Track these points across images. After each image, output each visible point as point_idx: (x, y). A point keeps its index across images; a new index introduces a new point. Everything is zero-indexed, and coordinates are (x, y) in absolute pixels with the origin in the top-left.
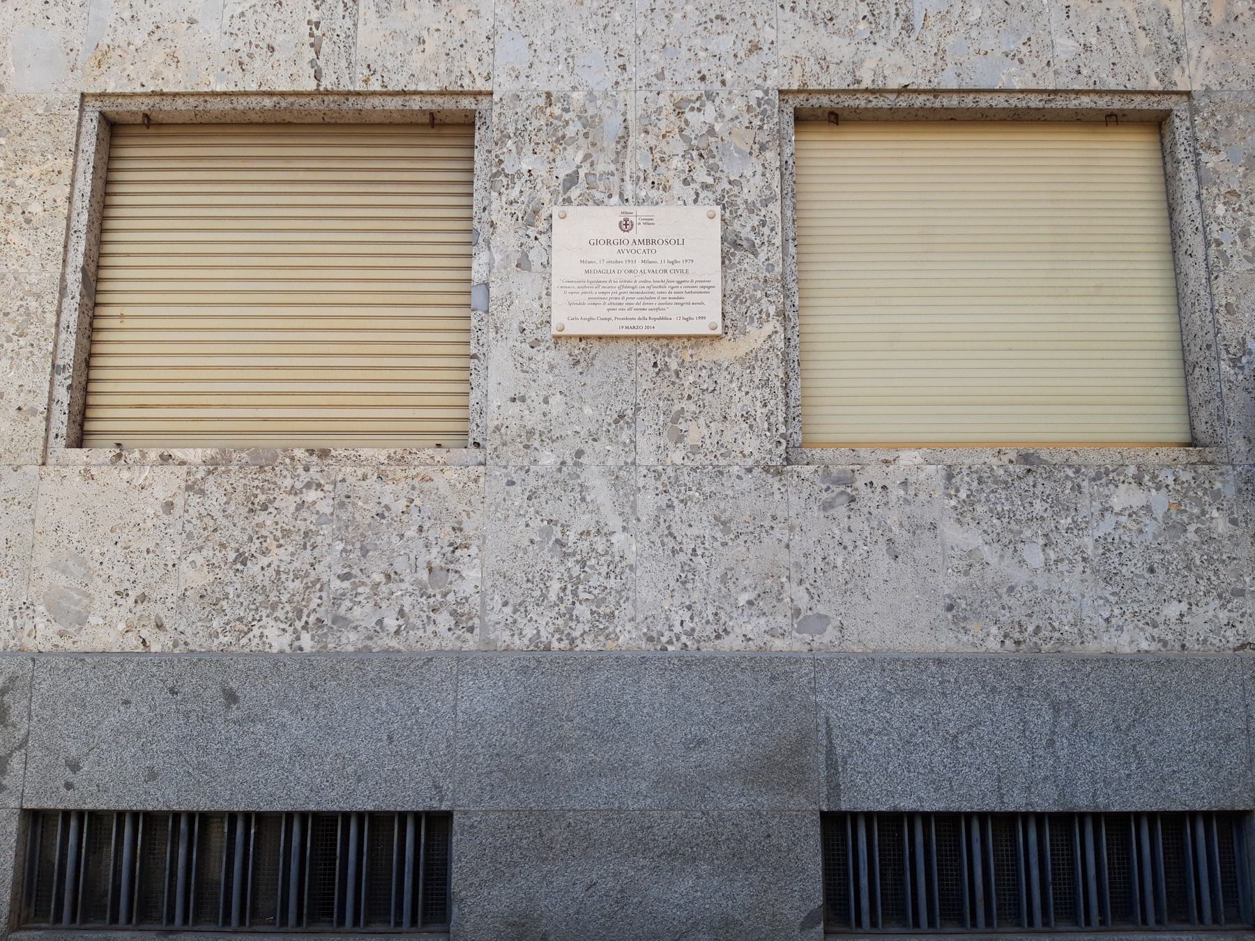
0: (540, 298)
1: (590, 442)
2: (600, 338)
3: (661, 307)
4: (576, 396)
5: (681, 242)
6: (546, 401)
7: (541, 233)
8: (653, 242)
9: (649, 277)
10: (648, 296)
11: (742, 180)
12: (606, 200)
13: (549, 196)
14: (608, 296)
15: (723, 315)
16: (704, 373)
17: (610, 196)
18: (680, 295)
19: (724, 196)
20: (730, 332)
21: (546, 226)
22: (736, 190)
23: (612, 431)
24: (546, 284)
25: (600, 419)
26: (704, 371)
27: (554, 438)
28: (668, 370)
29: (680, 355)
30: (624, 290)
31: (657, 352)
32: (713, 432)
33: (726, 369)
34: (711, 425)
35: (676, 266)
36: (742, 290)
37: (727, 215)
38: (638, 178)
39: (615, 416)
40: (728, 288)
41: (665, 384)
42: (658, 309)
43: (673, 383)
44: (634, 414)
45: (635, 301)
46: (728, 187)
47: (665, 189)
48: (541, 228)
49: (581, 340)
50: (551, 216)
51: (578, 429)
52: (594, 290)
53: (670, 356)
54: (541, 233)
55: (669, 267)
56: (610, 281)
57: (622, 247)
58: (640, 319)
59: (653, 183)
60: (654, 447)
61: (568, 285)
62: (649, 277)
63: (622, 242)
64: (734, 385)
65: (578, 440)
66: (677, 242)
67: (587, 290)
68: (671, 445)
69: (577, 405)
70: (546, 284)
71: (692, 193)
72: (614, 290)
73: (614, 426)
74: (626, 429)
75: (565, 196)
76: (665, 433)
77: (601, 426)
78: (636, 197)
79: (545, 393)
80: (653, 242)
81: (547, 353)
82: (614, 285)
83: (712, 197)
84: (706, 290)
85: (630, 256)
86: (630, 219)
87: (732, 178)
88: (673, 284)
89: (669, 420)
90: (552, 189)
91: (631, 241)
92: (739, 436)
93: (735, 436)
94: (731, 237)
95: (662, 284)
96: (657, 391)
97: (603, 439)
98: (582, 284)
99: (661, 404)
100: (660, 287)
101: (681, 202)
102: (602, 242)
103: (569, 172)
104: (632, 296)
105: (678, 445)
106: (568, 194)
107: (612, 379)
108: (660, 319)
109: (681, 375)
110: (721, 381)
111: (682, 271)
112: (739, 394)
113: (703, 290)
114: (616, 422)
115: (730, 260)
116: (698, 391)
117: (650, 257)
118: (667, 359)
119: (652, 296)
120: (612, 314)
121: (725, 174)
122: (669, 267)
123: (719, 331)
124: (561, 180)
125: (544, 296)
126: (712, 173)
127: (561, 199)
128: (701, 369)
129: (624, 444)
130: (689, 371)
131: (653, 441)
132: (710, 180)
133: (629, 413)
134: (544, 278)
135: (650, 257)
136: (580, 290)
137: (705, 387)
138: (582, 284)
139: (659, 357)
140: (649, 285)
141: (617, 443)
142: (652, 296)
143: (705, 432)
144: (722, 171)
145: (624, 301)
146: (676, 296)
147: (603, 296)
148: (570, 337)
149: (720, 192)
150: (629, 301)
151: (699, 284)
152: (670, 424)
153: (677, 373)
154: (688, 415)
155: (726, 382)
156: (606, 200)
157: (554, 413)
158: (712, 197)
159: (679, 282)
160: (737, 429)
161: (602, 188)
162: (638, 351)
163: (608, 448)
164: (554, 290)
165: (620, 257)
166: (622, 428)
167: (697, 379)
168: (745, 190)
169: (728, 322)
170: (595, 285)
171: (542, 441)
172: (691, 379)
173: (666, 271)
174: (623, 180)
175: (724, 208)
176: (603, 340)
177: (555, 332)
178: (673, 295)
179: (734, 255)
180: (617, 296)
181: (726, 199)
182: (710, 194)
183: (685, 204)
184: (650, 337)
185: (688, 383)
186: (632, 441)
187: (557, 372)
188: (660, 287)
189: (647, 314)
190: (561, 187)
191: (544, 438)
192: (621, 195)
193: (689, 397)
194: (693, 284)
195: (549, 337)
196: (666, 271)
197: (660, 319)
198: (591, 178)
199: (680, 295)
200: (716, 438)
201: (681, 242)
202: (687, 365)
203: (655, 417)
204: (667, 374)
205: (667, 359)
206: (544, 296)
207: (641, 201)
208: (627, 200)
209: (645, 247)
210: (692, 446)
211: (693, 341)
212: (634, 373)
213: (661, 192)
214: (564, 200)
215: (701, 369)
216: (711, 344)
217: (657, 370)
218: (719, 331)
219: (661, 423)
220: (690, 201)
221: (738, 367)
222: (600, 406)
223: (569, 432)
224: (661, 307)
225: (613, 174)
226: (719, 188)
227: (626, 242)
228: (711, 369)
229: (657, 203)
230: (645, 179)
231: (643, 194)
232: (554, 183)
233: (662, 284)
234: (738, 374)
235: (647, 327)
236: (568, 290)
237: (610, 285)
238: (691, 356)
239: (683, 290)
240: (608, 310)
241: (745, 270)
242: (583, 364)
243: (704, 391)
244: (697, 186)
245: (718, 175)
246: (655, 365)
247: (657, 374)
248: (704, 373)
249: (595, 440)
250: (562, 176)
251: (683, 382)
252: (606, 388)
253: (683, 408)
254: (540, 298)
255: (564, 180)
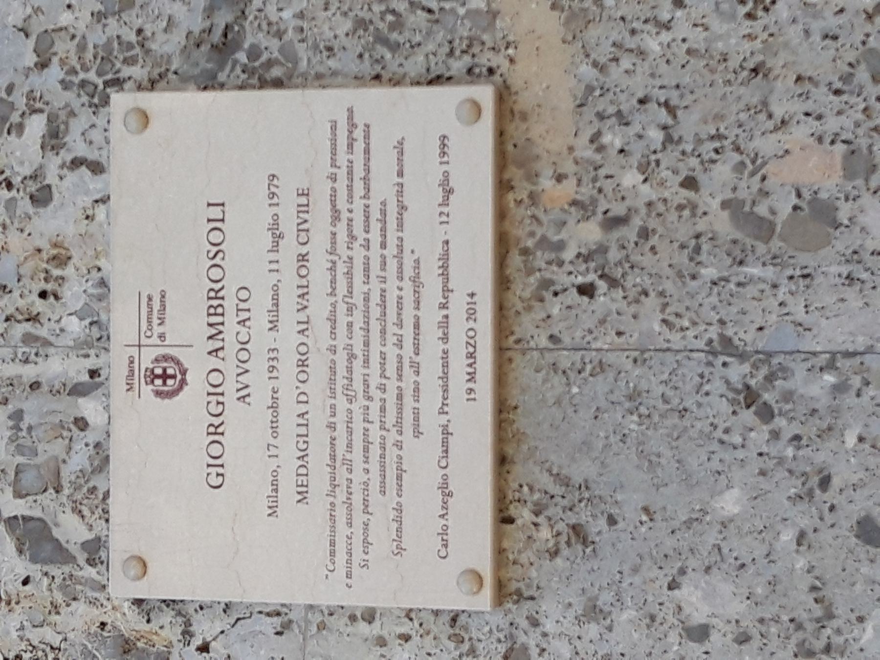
0: (382, 642)
1: (830, 496)
2: (502, 461)
3: (408, 272)
4: (686, 538)
5: (216, 213)
6: (700, 633)
7: (187, 634)
8: (216, 294)
9: (319, 307)
10: (375, 312)
11: (36, 29)
12: (91, 437)
13: (80, 607)
14: (375, 433)
15: (436, 80)
16: (613, 139)
17: (82, 424)
18: (375, 214)
19: (83, 84)
20: (486, 59)
21: (167, 617)
22: (63, 47)
23: (795, 429)
24: (339, 622)
25: (756, 464)
26: (607, 139)
27: (818, 611)
28: (602, 249)
29: (556, 215)
30: (358, 385)
31: (546, 284)
32: (798, 107)
33: (602, 69)
34: (779, 111)
35: (289, 227)
36: (361, 24)
37: (137, 72)
38: (28, 339)
39: (748, 416)
40: (354, 67)
41: (647, 260)
42: (416, 280)
43: (645, 233)
44: (742, 357)
45: (392, 352)
46: (55, 72)
47: (61, 260)
48: (173, 634)
49: (510, 520)
50: (139, 602)
51: (788, 536)
52: (358, 476)
53: (560, 246)
54: (187, 634)
55: (290, 248)
56: (332, 427)
57: (230, 388)
58: (445, 338)
59: (43, 295)
60: (850, 293)
61: (341, 557)
62: (319, 307)
63: (215, 391)
64: (653, 44)
65: (826, 535)
66: (216, 224)
67: (357, 499)
68: (843, 242)
69: (712, 537)
70: (339, 622)
71: (71, 177)
72: (358, 416)
73: (780, 422)
74: (789, 385)
75: (81, 558)
76: (804, 258)
77: (781, 461)
78: (83, 347)
79: (673, 637)
80: (216, 294)
81: (549, 626)
82: (341, 419)
83: (84, 118)
84: (359, 133)
85: (258, 365)
86: (147, 363)
87: (31, 59)
88: (342, 237)
89: (761, 248)
90: (59, 597)
91: (213, 362)
92: (817, 27)
93: (816, 38)
94: (203, 59)
95: (341, 268)
96: (668, 286)
97: (820, 458)
98: (341, 513)
99: (709, 273)
100: (349, 274)
101: (101, 212)
102: (215, 450)
103: (10, 546)
104: (375, 359)
105: (843, 216)
106: (74, 550)
107: (632, 423)
108: (445, 274)
109: (619, 209)
110: (639, 85)
111: (303, 209)
112: (682, 29)
113: (360, 146)
114: (766, 414)
115: (270, 63)
116: (668, 159)
117: (261, 303)
118: (569, 255)
119: (375, 298)
120: (431, 423)
121: (18, 80)
122: (290, 248)
123: (485, 94)
124: (34, 570)
125: (375, 629)
126: (15, 118)
127: (90, 572)
128: (601, 149)
129: (839, 389)
130: (608, 185)
131: (829, 299)
132: (37, 126)
133: (737, 372)
134: (321, 627)
135: (261, 303)
136: (359, 518)
137: (656, 136)
138: (341, 513)
139: (562, 279)
140: (342, 308)
141: (835, 411)
142: (375, 298)
143: (800, 133)
144: (10, 89)
145: (392, 386)
146: (375, 227)
147: (375, 451)
148: (499, 552)
149: (69, 96)
150: (391, 371)
151: (342, 158)
152: (776, 244)
153: (613, 222)
154: (748, 187)
155: (643, 68)
156: (91, 437)
157: (737, 608)
158: (84, 118)
159: (336, 216)
160: (794, 33)
161: (57, 448)
162: (544, 342)
163: (851, 440)
164: (358, 600)
165: (260, 396)
166: (787, 396)
167: (634, 160)
168: (66, 18)
169: (458, 66)
170: (342, 473)
171: (828, 649)
172: (631, 178)
173: (303, 258)
174: (35, 386)
175: (117, 83)
176: (510, 450)
177: (484, 600)
178: (375, 236)
179: (254, 53)
180: (375, 406)
181: (92, 76)
182: (77, 126)
183: (104, 200)
184: (501, 309)
185: (645, 189)
186: (830, 366)
187: (605, 598)
188: (349, 274)
189: (431, 317)
190: (55, 571)
191: (819, 645)
192: (78, 391)
193: (690, 183)
194: (342, 173)
195: (498, 619)
196: (303, 258)
197: (445, 274)
198: (29, 479)
199: (375, 214)
200: (822, 98)
201: (216, 213)
202: (586, 192)
203: (751, 291)
204: (614, 255)
205: (569, 255)
206: (375, 629)
207: (95, 332)
208: (93, 373)
209: (231, 320)
210: (849, 173)
211: (514, 173)
212: (610, 358)
213: (69, 271)
214: (91, 562)
215: (601, 149)
216: (524, 117)
217: (602, 285)
218: (485, 94)
219: (770, 272)
220: (96, 185)
221: (593, 33)
222: (715, 465)
223: (801, 563)
224: (408, 272)
225: (18, 416)
226: (60, 98)
227: (215, 378)
228: (601, 116)
229: (103, 283)
230: (33, 319)
231: (75, 326)
232: (40, 588)
233: (341, 268)
234: (618, 33)
235: (471, 314)
236: (358, 555)
237: (341, 428)
238: (560, 178)
239: (358, 204)
240: (417, 433)
241: (301, 15)
242: (583, 516)
243: (669, 140)
244: (53, 163)
245: (20, 101)
246: (586, 290)
247: (613, 283)
248: (613, 139)
249: (825, 483)
250: (23, 567)
251: (640, 203)
252: (656, 442)
253: (725, 205)
254: (382, 642)
255: (34, 560)
